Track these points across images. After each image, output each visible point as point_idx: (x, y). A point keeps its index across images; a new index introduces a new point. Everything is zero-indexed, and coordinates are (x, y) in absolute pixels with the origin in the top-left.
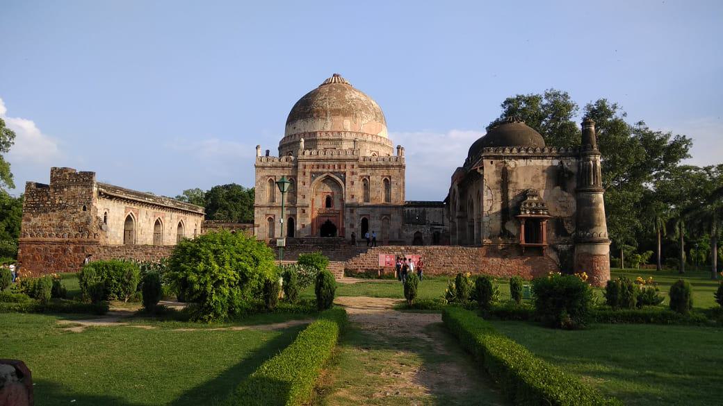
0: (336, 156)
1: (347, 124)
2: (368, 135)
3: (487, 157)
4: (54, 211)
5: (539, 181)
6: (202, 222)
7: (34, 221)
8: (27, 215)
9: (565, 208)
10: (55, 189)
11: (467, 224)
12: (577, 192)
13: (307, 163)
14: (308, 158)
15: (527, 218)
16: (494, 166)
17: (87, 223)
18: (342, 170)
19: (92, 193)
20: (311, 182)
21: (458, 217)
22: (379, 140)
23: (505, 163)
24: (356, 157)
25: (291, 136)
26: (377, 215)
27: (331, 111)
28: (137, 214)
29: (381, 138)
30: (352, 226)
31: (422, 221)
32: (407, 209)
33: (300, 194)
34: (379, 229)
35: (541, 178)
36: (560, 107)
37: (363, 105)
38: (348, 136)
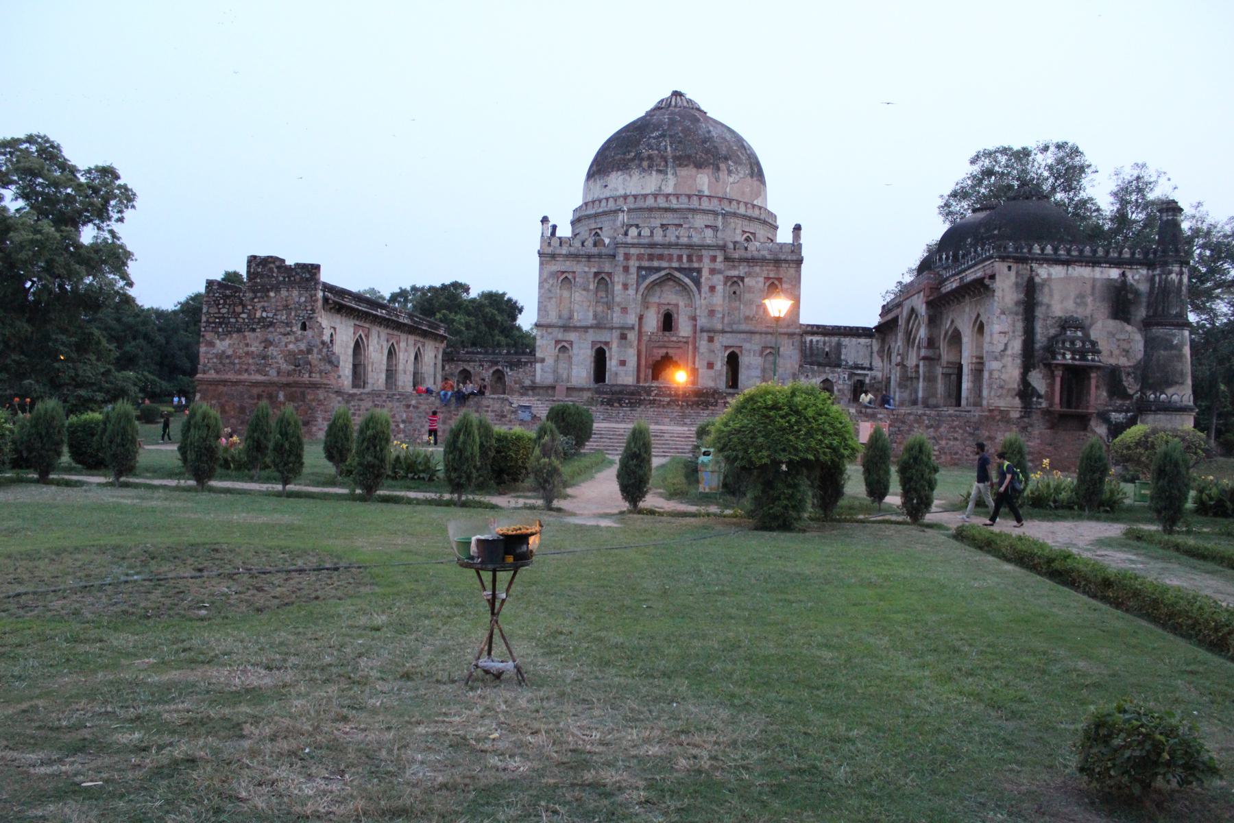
0: (684, 240)
1: (703, 181)
2: (739, 202)
3: (1003, 259)
4: (254, 330)
5: (1085, 304)
6: (445, 353)
7: (222, 345)
8: (209, 336)
9: (1126, 352)
10: (254, 292)
11: (939, 371)
12: (1147, 325)
13: (633, 251)
14: (636, 241)
15: (1067, 368)
16: (1013, 273)
17: (309, 351)
18: (696, 265)
19: (316, 301)
20: (638, 285)
21: (924, 358)
22: (756, 213)
23: (1032, 270)
24: (721, 243)
25: (600, 201)
26: (757, 348)
27: (675, 158)
28: (367, 336)
29: (760, 208)
30: (710, 366)
31: (831, 360)
32: (808, 338)
33: (618, 305)
34: (758, 373)
35: (1089, 300)
36: (1070, 169)
37: (730, 148)
38: (705, 204)
